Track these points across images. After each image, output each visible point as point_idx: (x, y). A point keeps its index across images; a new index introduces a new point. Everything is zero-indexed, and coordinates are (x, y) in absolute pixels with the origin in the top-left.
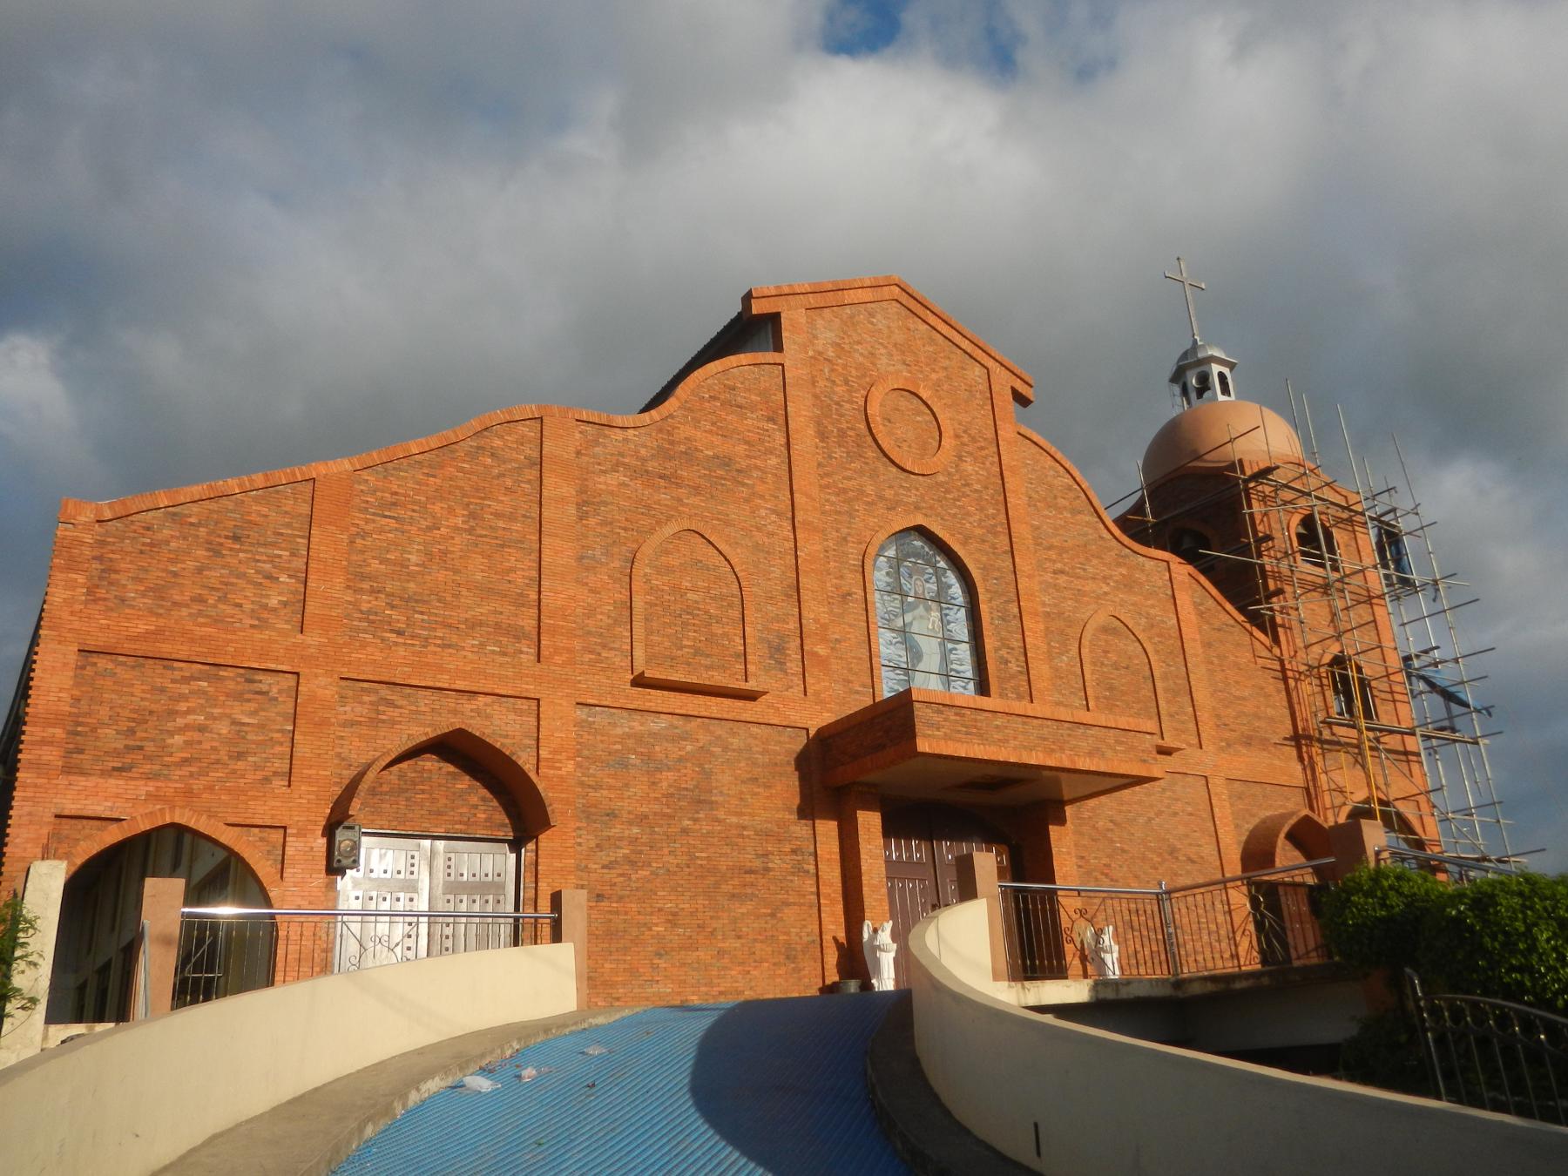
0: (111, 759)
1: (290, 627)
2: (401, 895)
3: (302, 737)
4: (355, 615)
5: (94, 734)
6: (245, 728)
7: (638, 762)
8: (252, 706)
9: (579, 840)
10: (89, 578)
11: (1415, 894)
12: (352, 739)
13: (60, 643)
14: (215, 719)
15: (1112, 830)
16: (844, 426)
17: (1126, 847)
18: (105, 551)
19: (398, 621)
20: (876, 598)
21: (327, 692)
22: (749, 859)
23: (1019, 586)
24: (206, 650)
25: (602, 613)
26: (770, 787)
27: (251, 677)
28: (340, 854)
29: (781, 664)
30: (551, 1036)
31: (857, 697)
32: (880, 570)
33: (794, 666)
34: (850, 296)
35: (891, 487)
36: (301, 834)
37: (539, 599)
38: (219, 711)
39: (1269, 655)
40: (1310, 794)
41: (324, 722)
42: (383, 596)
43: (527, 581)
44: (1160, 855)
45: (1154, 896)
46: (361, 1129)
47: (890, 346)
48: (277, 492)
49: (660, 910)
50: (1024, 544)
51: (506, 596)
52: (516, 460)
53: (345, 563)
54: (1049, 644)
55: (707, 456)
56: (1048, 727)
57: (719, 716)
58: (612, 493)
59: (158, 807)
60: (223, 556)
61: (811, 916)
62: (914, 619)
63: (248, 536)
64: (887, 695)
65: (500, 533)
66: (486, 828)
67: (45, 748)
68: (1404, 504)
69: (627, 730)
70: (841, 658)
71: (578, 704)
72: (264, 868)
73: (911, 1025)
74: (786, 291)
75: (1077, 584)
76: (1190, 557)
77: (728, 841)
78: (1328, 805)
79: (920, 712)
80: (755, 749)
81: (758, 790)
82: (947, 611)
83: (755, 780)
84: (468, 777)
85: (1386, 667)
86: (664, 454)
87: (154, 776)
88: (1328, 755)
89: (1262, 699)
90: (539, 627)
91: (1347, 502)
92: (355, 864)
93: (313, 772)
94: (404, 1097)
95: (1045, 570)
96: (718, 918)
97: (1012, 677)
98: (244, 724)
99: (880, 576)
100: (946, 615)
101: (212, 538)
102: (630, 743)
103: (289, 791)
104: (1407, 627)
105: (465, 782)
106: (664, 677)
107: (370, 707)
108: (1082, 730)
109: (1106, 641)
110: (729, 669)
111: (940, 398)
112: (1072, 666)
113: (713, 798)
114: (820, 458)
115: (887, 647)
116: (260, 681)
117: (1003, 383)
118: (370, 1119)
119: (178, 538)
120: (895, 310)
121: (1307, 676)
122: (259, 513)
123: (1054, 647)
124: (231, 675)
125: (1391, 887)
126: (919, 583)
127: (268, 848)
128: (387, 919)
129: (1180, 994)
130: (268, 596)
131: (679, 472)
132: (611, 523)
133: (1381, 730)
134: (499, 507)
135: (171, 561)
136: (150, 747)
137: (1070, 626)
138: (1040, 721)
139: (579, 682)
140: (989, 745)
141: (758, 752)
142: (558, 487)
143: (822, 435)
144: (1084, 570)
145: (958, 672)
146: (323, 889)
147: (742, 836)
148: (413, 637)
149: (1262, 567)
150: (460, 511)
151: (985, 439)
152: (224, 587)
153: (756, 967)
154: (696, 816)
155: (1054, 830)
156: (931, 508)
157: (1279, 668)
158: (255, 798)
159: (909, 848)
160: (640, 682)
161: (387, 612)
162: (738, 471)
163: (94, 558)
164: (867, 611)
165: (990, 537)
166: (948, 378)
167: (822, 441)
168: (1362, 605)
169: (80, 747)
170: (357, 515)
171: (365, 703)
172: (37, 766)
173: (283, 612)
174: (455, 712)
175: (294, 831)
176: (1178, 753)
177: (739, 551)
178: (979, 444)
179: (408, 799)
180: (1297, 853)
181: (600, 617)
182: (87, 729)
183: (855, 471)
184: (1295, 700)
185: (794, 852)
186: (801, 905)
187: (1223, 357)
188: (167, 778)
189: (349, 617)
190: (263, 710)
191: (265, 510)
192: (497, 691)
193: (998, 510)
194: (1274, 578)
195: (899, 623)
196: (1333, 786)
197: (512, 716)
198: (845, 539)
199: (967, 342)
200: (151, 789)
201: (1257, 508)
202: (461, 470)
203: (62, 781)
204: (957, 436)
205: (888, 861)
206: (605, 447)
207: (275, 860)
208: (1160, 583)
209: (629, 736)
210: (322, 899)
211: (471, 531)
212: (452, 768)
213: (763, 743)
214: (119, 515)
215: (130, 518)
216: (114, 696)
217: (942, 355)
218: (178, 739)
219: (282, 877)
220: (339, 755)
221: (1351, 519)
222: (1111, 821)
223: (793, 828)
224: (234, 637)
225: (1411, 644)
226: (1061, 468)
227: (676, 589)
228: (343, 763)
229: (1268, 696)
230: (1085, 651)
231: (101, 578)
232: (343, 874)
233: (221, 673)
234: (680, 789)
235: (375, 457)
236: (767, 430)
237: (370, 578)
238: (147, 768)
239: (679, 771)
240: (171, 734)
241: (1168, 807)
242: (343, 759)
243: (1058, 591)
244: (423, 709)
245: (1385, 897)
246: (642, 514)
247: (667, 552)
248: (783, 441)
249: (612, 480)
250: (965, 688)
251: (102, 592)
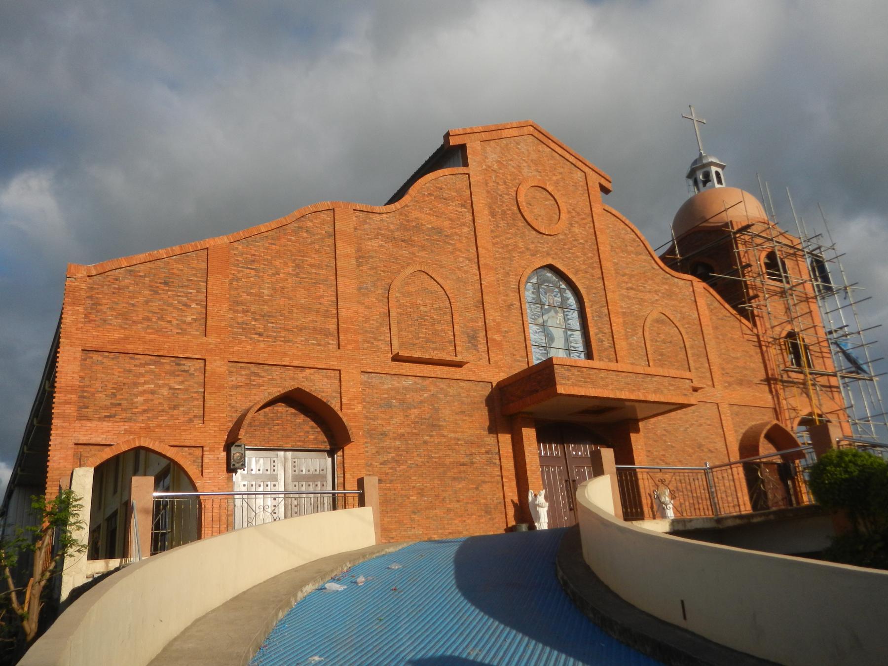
0: (103, 411)
1: (198, 333)
2: (269, 483)
3: (209, 396)
4: (235, 325)
5: (94, 398)
6: (177, 391)
7: (397, 404)
8: (180, 379)
9: (366, 449)
10: (86, 309)
11: (865, 465)
12: (238, 396)
13: (71, 346)
14: (160, 387)
16: (505, 208)
17: (674, 445)
18: (93, 293)
19: (259, 328)
20: (526, 306)
21: (221, 369)
22: (462, 457)
23: (608, 298)
24: (153, 348)
25: (373, 320)
26: (472, 416)
27: (179, 362)
28: (234, 460)
29: (475, 346)
30: (366, 560)
31: (518, 363)
32: (528, 290)
33: (482, 347)
34: (505, 133)
35: (533, 243)
36: (212, 450)
37: (338, 313)
38: (162, 382)
39: (751, 333)
40: (777, 412)
41: (221, 387)
42: (250, 314)
43: (330, 303)
44: (693, 448)
45: (703, 471)
46: (277, 614)
47: (529, 162)
48: (188, 256)
49: (414, 487)
50: (610, 273)
51: (318, 312)
52: (321, 234)
53: (228, 296)
54: (626, 330)
55: (428, 228)
56: (630, 377)
57: (442, 376)
58: (375, 251)
59: (132, 437)
60: (159, 294)
61: (498, 488)
63: (173, 282)
64: (536, 362)
65: (314, 276)
66: (314, 444)
67: (67, 406)
68: (825, 243)
69: (390, 386)
70: (509, 342)
71: (362, 372)
72: (192, 470)
73: (580, 547)
74: (469, 131)
75: (640, 295)
76: (704, 278)
77: (450, 447)
78: (787, 417)
79: (558, 370)
80: (463, 395)
81: (465, 418)
82: (567, 313)
83: (463, 412)
84: (303, 415)
85: (818, 338)
86: (403, 227)
87: (129, 420)
88: (787, 389)
89: (748, 358)
90: (338, 329)
91: (792, 244)
92: (243, 466)
93: (217, 415)
94: (295, 595)
95: (622, 288)
96: (447, 491)
97: (606, 349)
98: (176, 389)
99: (528, 294)
100: (567, 315)
101: (153, 284)
102: (392, 393)
103: (204, 426)
104: (829, 314)
105: (301, 418)
106: (410, 355)
107: (246, 377)
108: (649, 378)
109: (658, 328)
110: (444, 349)
111: (558, 191)
112: (640, 342)
113: (441, 423)
114: (492, 227)
115: (534, 335)
116: (184, 365)
117: (594, 180)
118: (280, 608)
119: (134, 284)
120: (531, 140)
121: (773, 344)
122: (179, 270)
123: (629, 332)
124: (168, 361)
125: (850, 461)
126: (551, 297)
127: (194, 459)
128: (262, 496)
129: (721, 527)
130: (185, 316)
131: (412, 238)
132: (376, 268)
133: (816, 374)
134: (312, 261)
135: (130, 297)
136: (125, 404)
137: (637, 320)
138: (626, 374)
139: (362, 359)
140: (598, 388)
141: (464, 397)
142: (345, 249)
143: (493, 214)
144: (644, 287)
145: (574, 347)
146: (226, 481)
147: (457, 444)
148: (268, 337)
149: (745, 282)
150: (290, 264)
151: (585, 214)
152: (161, 311)
153: (469, 518)
154: (431, 433)
155: (633, 436)
156: (556, 254)
157: (756, 340)
158: (185, 431)
159: (551, 449)
160: (396, 358)
161: (253, 323)
162: (445, 236)
163: (88, 297)
164: (522, 314)
165: (590, 270)
166: (563, 179)
167: (493, 217)
168: (804, 303)
169: (86, 405)
170: (233, 268)
171: (243, 375)
172: (64, 416)
173: (194, 325)
174: (293, 379)
175: (208, 449)
176: (701, 390)
177: (448, 282)
179: (270, 429)
180: (770, 446)
181: (372, 322)
182: (89, 394)
183: (512, 234)
184: (766, 358)
185: (487, 452)
186: (491, 482)
187: (718, 162)
188: (135, 421)
189: (231, 326)
190: (186, 381)
191: (181, 267)
192: (316, 366)
193: (594, 254)
194: (752, 289)
195: (540, 321)
196: (790, 407)
197: (325, 380)
198: (508, 273)
199: (573, 157)
200: (127, 427)
201: (741, 248)
202: (290, 240)
203: (77, 424)
204: (569, 212)
205: (540, 456)
206: (371, 225)
207: (198, 465)
208: (687, 293)
209: (392, 389)
210: (226, 486)
211: (297, 275)
212: (293, 411)
213: (467, 391)
214: (100, 272)
215: (106, 274)
216: (104, 376)
217: (559, 166)
218: (140, 399)
219: (202, 475)
220: (230, 405)
221: (795, 253)
222: (665, 430)
223: (485, 439)
224: (169, 340)
225: (832, 324)
226: (629, 229)
227: (414, 305)
228: (233, 410)
229: (751, 356)
230: (646, 334)
231: (92, 309)
232: (236, 472)
233: (162, 360)
234: (422, 419)
235: (242, 235)
236: (462, 212)
237: (242, 303)
238: (124, 415)
239: (420, 408)
240: (136, 396)
241: (697, 421)
242: (233, 407)
243: (630, 299)
244: (276, 377)
245: (847, 467)
246: (393, 262)
247: (408, 284)
248: (471, 218)
249: (375, 243)
250: (579, 357)
251: (92, 317)
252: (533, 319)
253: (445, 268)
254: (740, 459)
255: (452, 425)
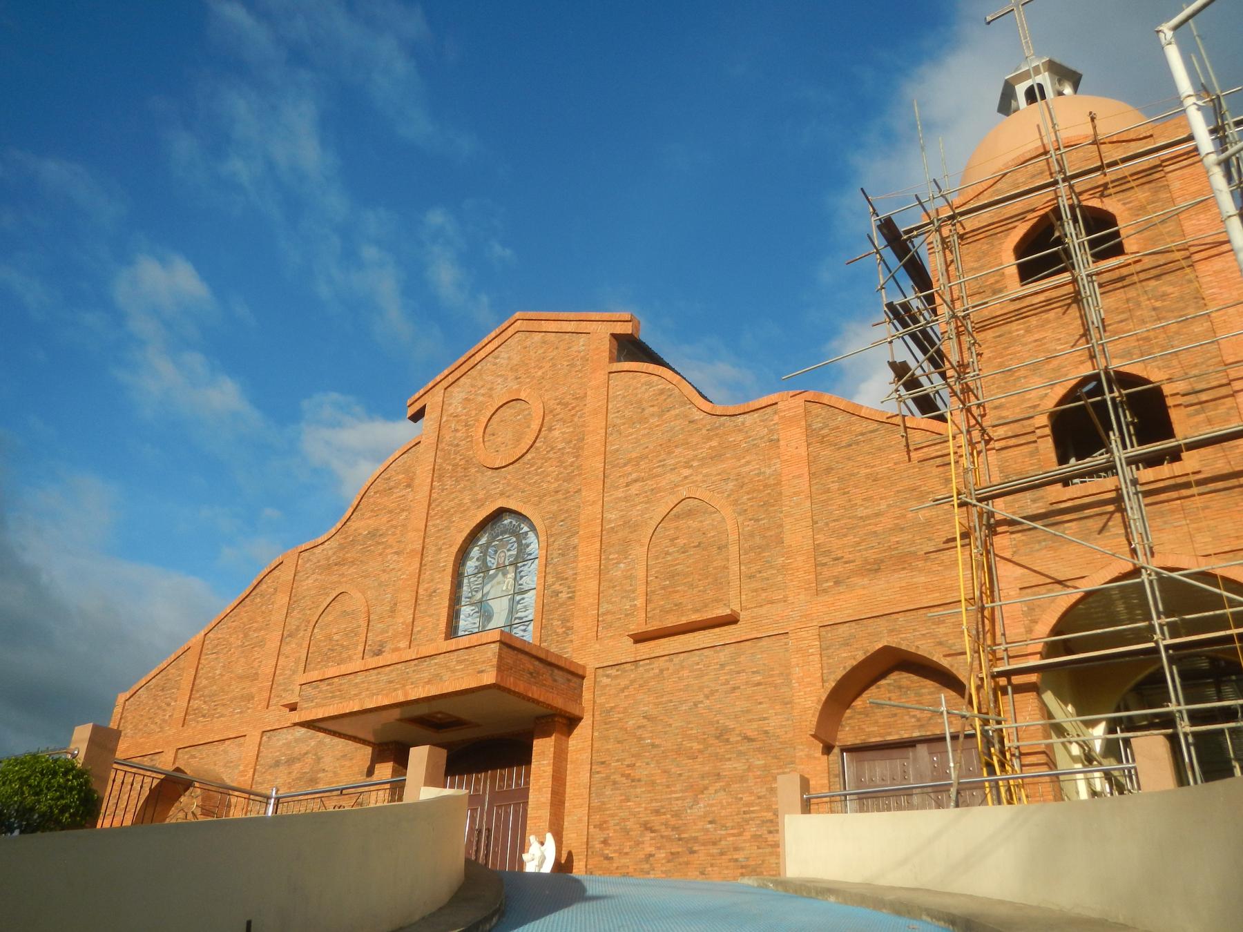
15: (644, 727)
17: (657, 742)
34: (478, 357)
58: (309, 589)
62: (492, 587)
115: (468, 619)
123: (613, 559)
126: (502, 554)
130: (165, 715)
145: (520, 618)
166: (554, 365)
178: (570, 407)
195: (479, 596)
209: (284, 744)
241: (727, 682)
243: (627, 501)
246: (321, 594)
249: (310, 581)
250: (525, 631)
252: (468, 598)
253: (369, 576)
254: (392, 777)
255: (330, 775)
